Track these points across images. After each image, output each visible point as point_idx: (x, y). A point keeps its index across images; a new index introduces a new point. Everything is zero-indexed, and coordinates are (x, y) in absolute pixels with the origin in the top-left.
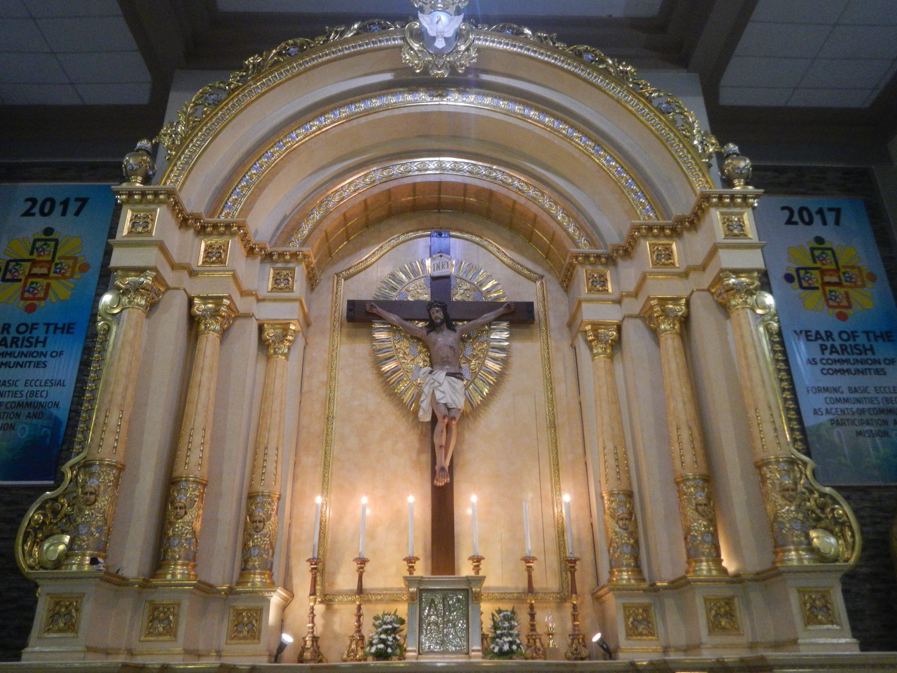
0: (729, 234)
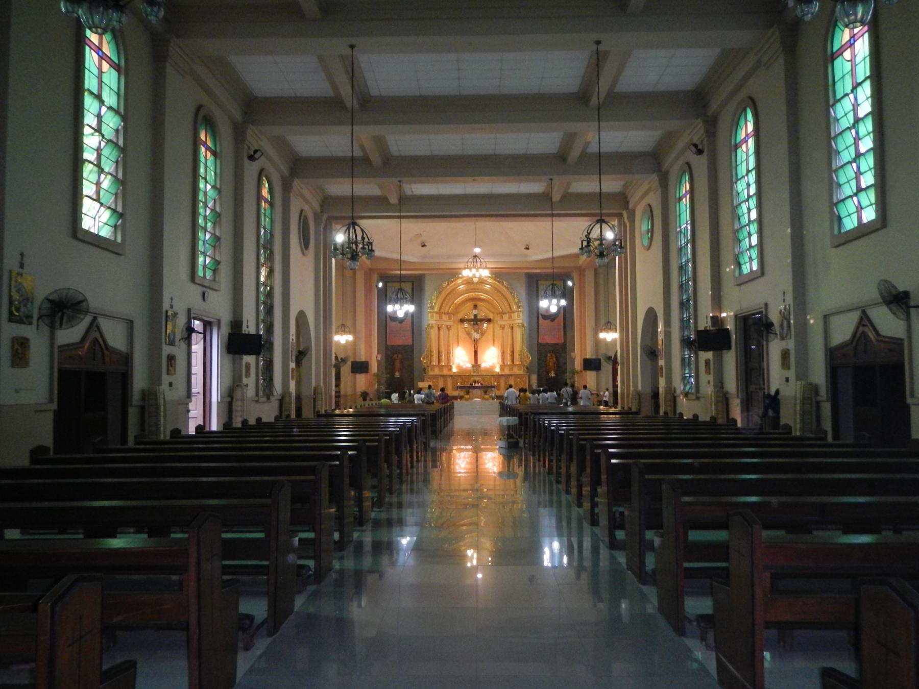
0: (518, 317)
